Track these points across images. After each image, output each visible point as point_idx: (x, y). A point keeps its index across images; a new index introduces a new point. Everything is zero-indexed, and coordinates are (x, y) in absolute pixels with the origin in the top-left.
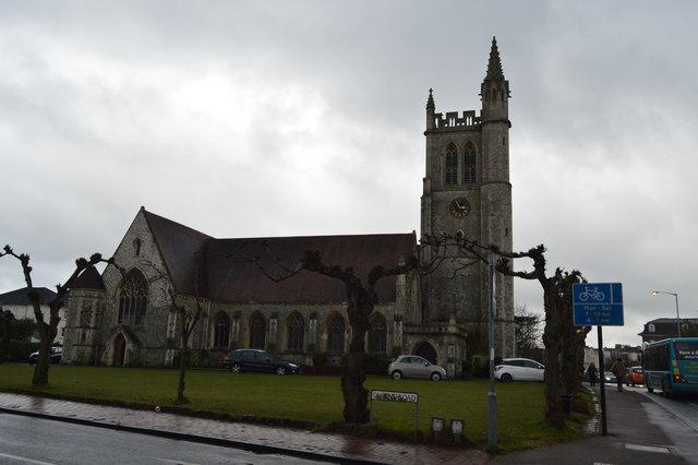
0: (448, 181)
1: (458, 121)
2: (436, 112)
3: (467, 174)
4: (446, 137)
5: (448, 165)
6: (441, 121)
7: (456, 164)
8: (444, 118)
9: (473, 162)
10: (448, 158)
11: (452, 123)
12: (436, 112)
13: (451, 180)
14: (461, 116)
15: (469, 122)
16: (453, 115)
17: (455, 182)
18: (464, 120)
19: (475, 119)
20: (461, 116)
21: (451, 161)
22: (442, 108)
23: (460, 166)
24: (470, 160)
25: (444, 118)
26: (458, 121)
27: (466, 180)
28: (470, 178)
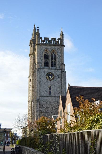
0: (45, 65)
1: (49, 41)
2: (40, 36)
3: (52, 62)
4: (45, 47)
5: (45, 58)
6: (42, 41)
7: (48, 58)
8: (43, 39)
9: (55, 59)
10: (45, 56)
11: (47, 42)
12: (40, 36)
13: (46, 64)
14: (50, 39)
15: (53, 42)
16: (47, 39)
17: (48, 66)
18: (51, 41)
19: (56, 41)
20: (50, 39)
21: (46, 57)
22: (43, 35)
23: (50, 58)
24: (54, 57)
25: (43, 39)
26: (49, 41)
27: (52, 66)
28: (54, 65)
